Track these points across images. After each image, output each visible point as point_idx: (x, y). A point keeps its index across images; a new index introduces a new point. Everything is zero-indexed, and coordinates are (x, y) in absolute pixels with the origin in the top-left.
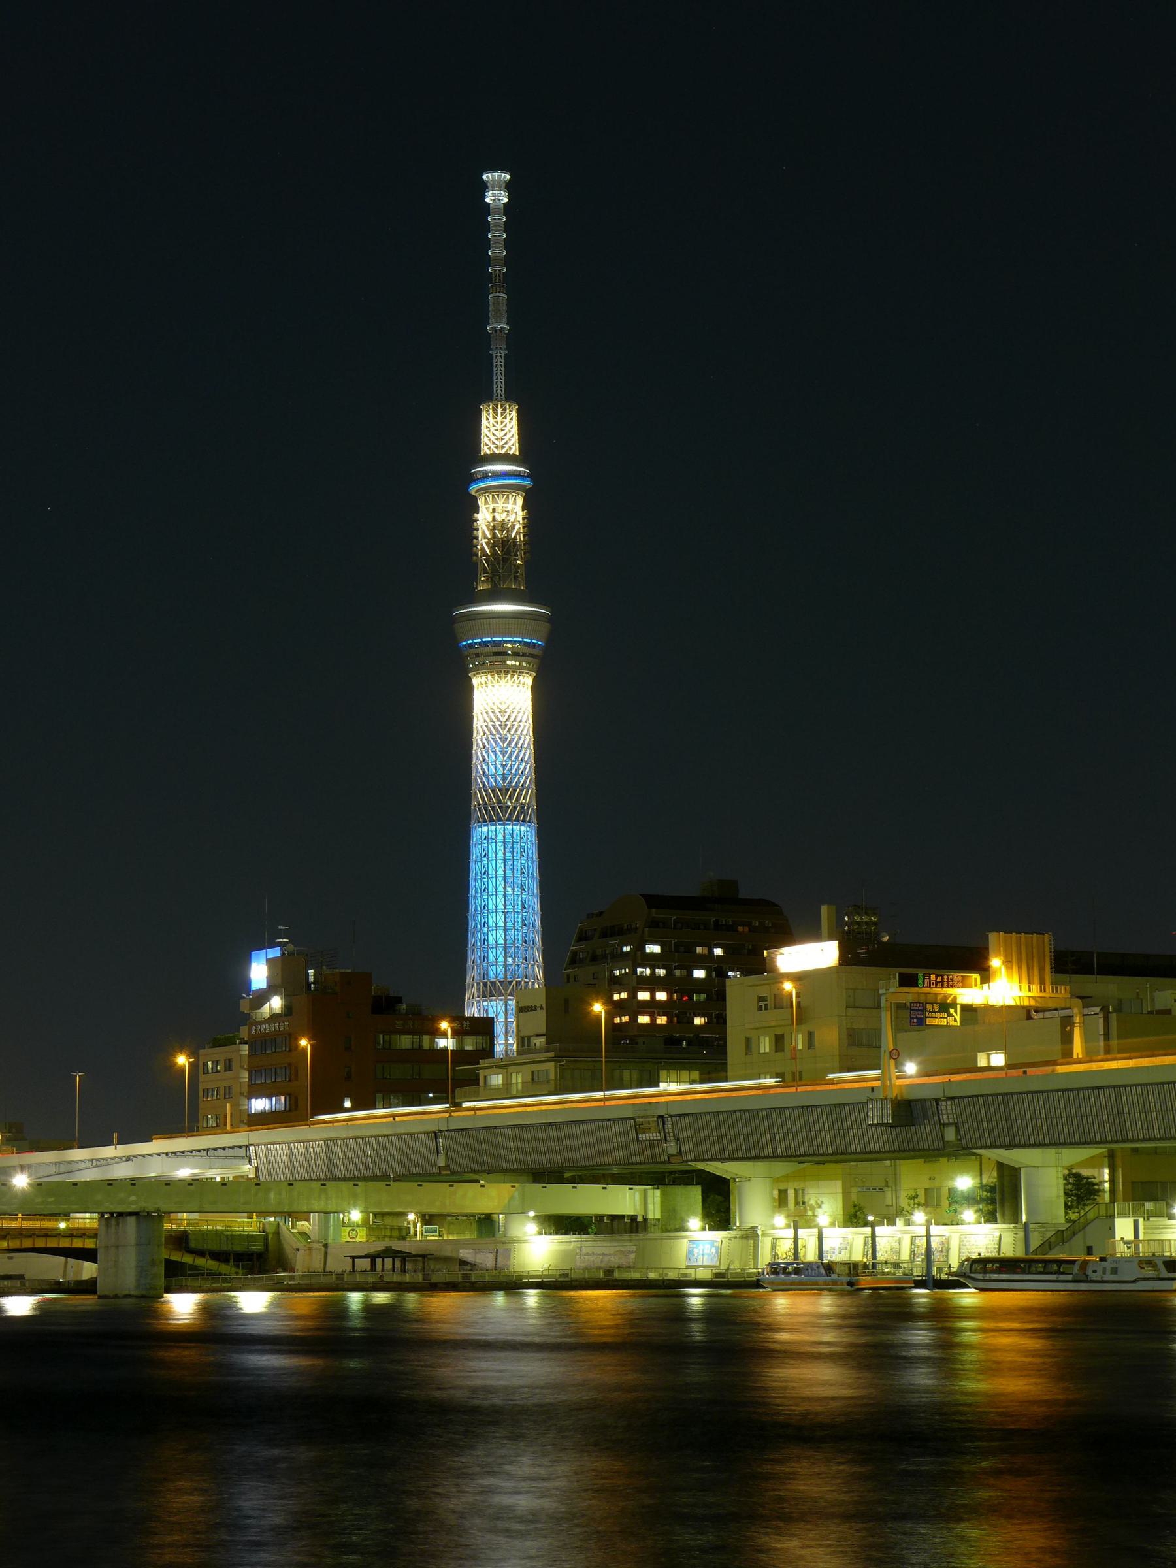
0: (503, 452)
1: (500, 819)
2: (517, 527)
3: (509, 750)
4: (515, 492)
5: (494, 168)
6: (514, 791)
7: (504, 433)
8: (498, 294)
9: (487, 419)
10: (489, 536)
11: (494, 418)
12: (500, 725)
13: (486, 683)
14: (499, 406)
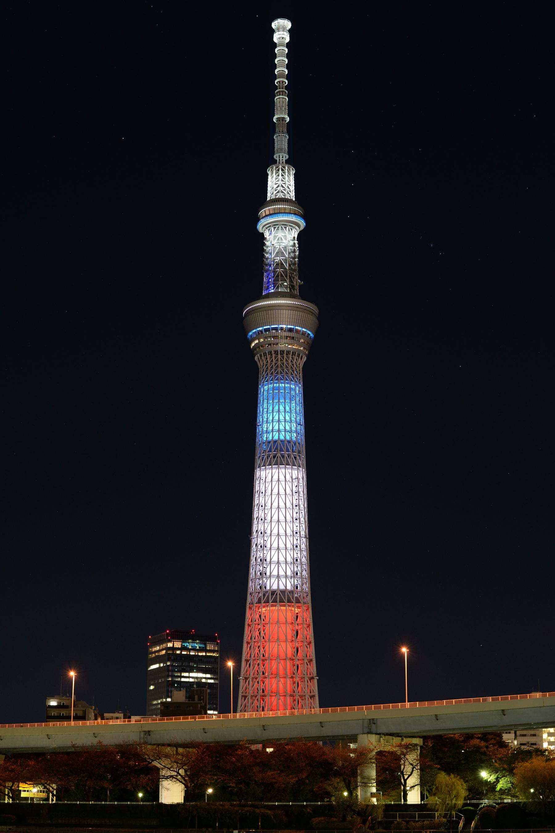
7: (277, 185)
8: (281, 96)
14: (274, 168)
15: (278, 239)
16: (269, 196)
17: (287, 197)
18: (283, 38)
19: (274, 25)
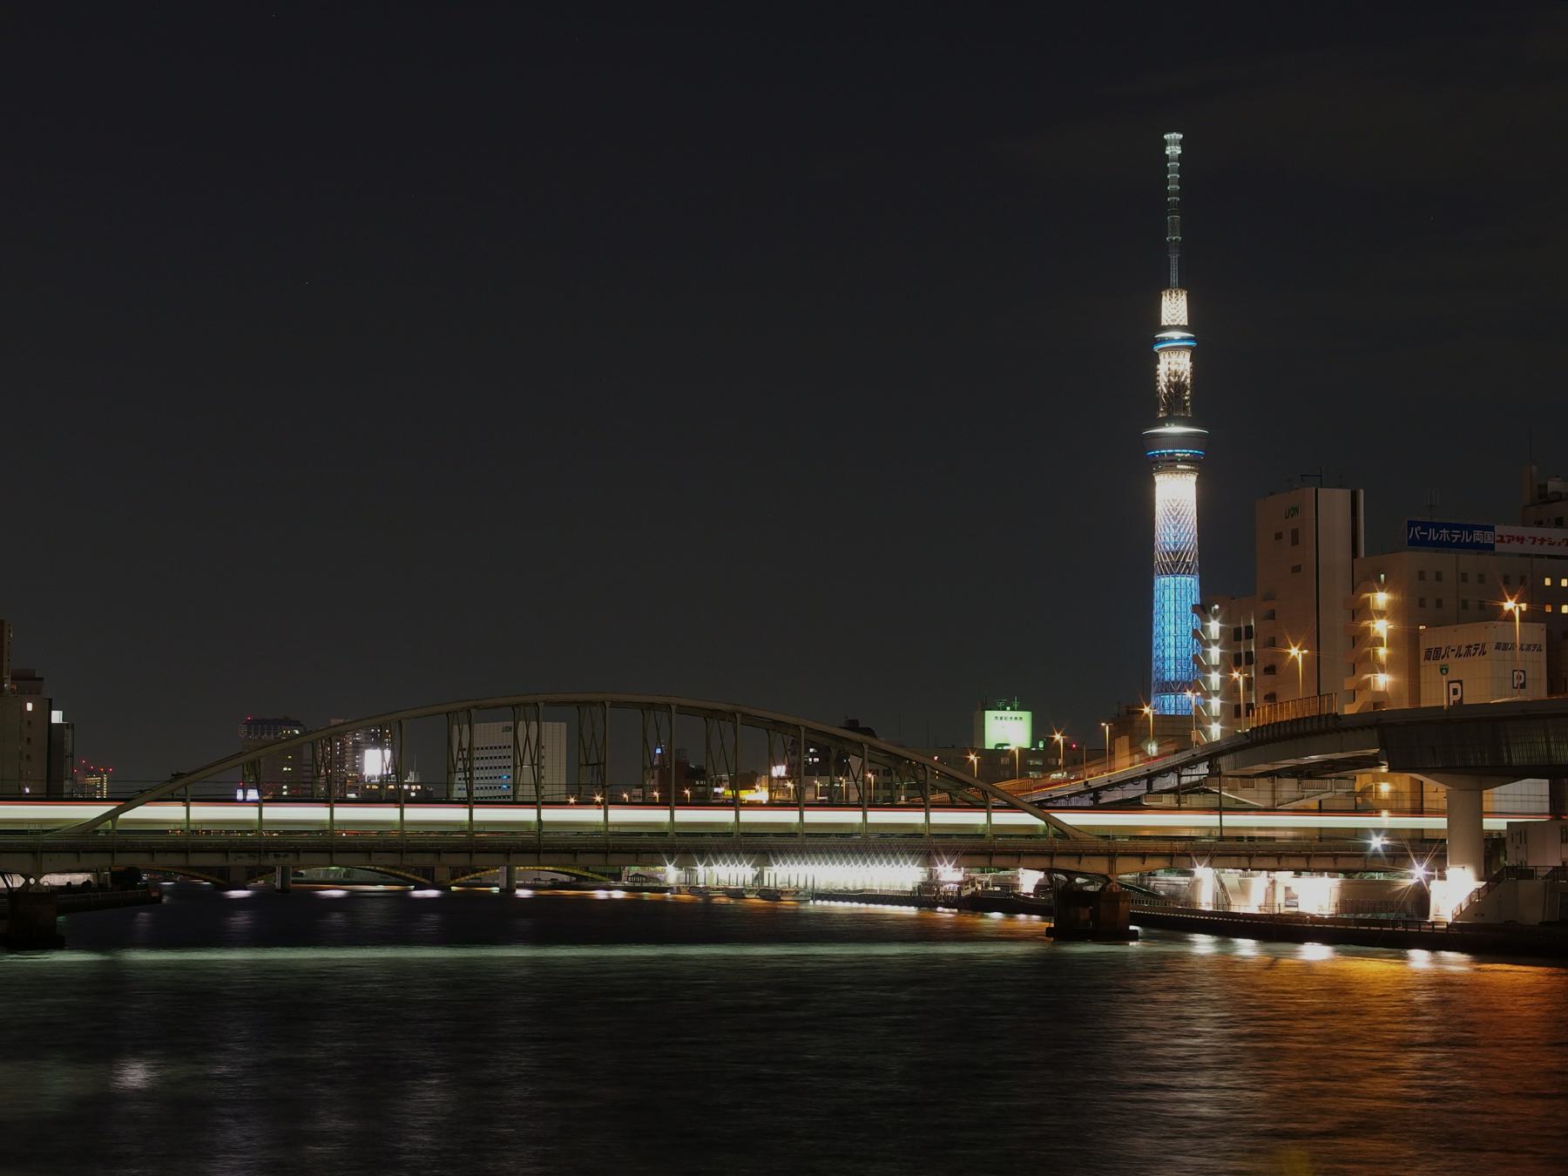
0: (1176, 323)
1: (1172, 573)
2: (1185, 375)
3: (1179, 526)
5: (1171, 131)
6: (1182, 553)
10: (1166, 381)
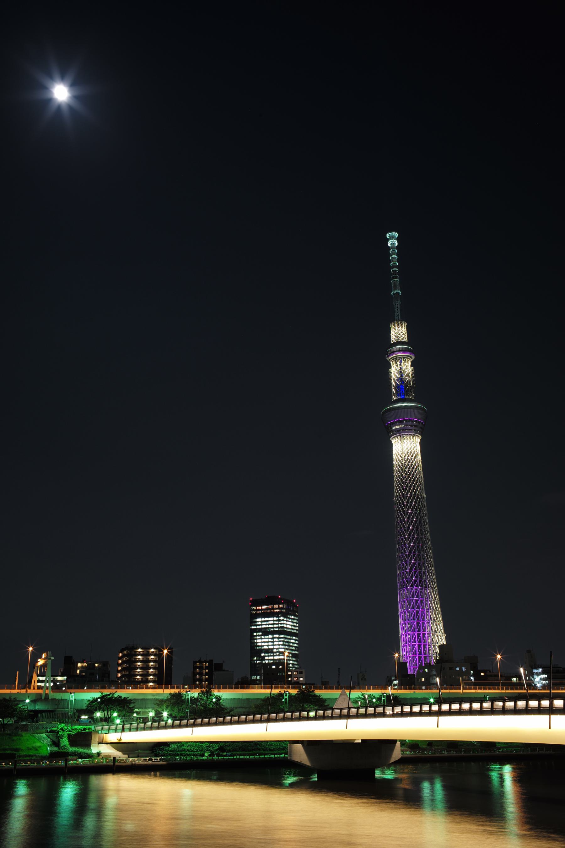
4: (405, 357)
8: (395, 280)
9: (392, 330)
11: (394, 328)
12: (402, 460)
13: (396, 442)
14: (396, 323)
15: (406, 366)
16: (393, 340)
17: (404, 340)
18: (393, 243)
19: (388, 236)
